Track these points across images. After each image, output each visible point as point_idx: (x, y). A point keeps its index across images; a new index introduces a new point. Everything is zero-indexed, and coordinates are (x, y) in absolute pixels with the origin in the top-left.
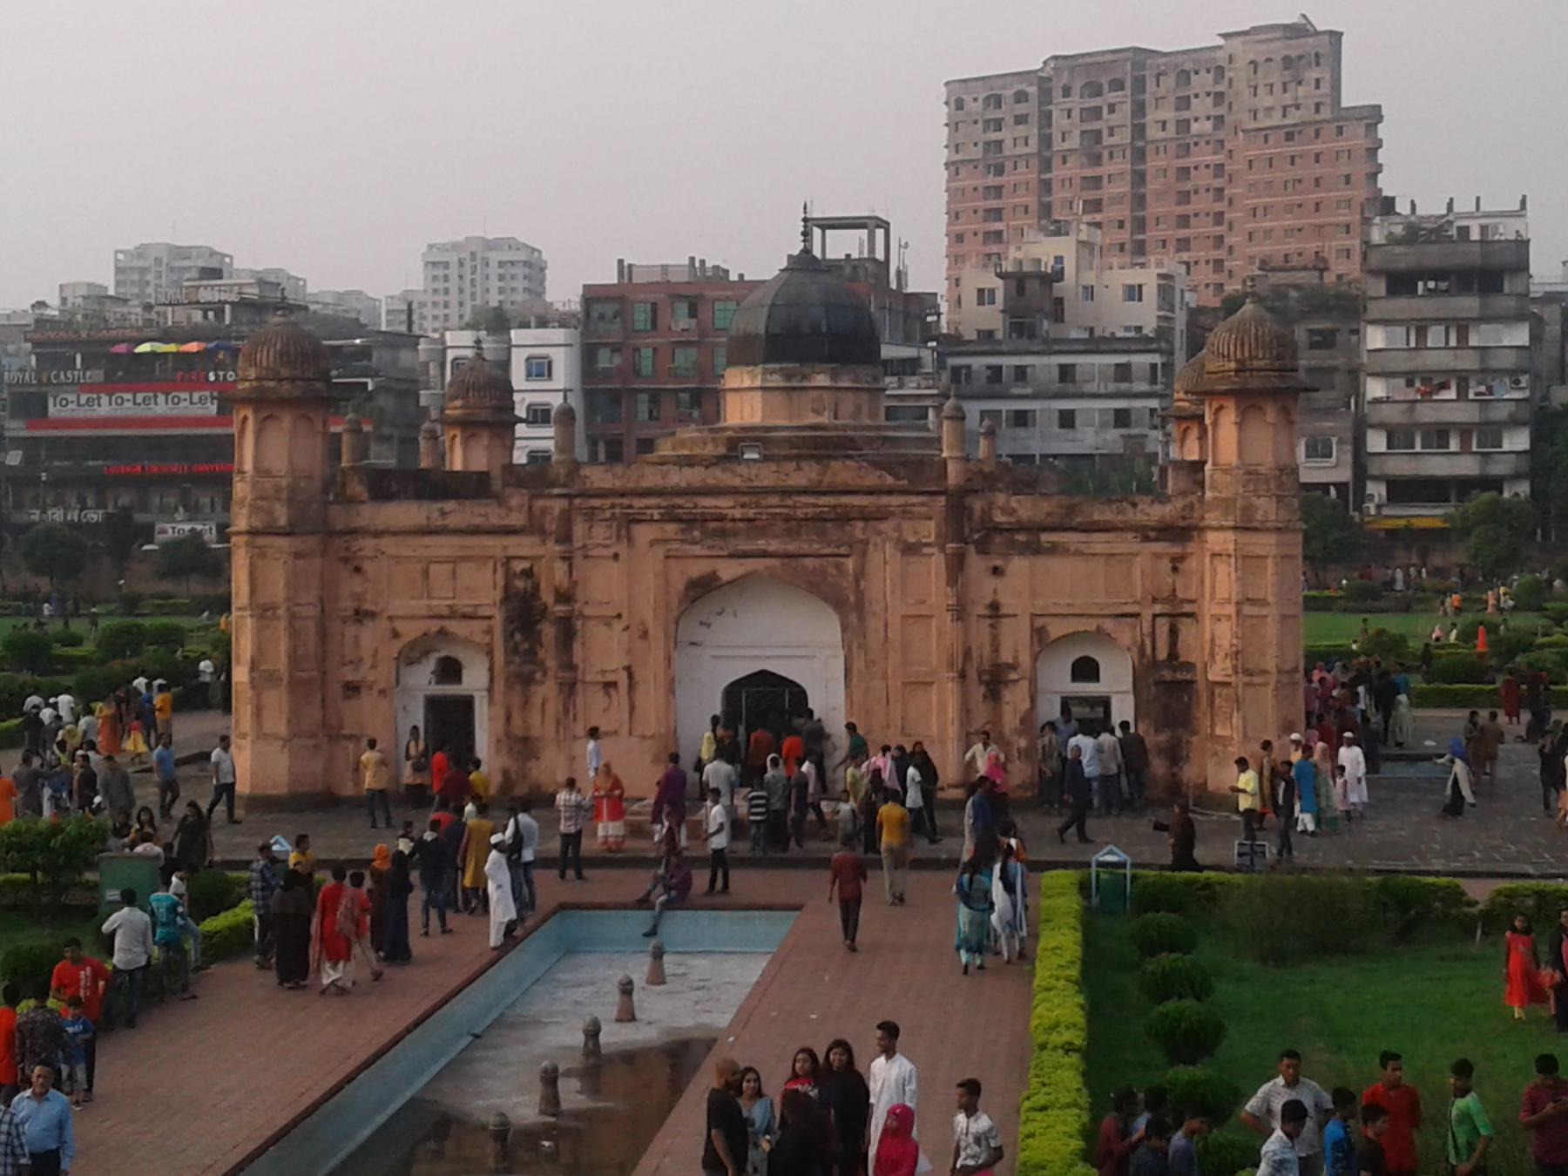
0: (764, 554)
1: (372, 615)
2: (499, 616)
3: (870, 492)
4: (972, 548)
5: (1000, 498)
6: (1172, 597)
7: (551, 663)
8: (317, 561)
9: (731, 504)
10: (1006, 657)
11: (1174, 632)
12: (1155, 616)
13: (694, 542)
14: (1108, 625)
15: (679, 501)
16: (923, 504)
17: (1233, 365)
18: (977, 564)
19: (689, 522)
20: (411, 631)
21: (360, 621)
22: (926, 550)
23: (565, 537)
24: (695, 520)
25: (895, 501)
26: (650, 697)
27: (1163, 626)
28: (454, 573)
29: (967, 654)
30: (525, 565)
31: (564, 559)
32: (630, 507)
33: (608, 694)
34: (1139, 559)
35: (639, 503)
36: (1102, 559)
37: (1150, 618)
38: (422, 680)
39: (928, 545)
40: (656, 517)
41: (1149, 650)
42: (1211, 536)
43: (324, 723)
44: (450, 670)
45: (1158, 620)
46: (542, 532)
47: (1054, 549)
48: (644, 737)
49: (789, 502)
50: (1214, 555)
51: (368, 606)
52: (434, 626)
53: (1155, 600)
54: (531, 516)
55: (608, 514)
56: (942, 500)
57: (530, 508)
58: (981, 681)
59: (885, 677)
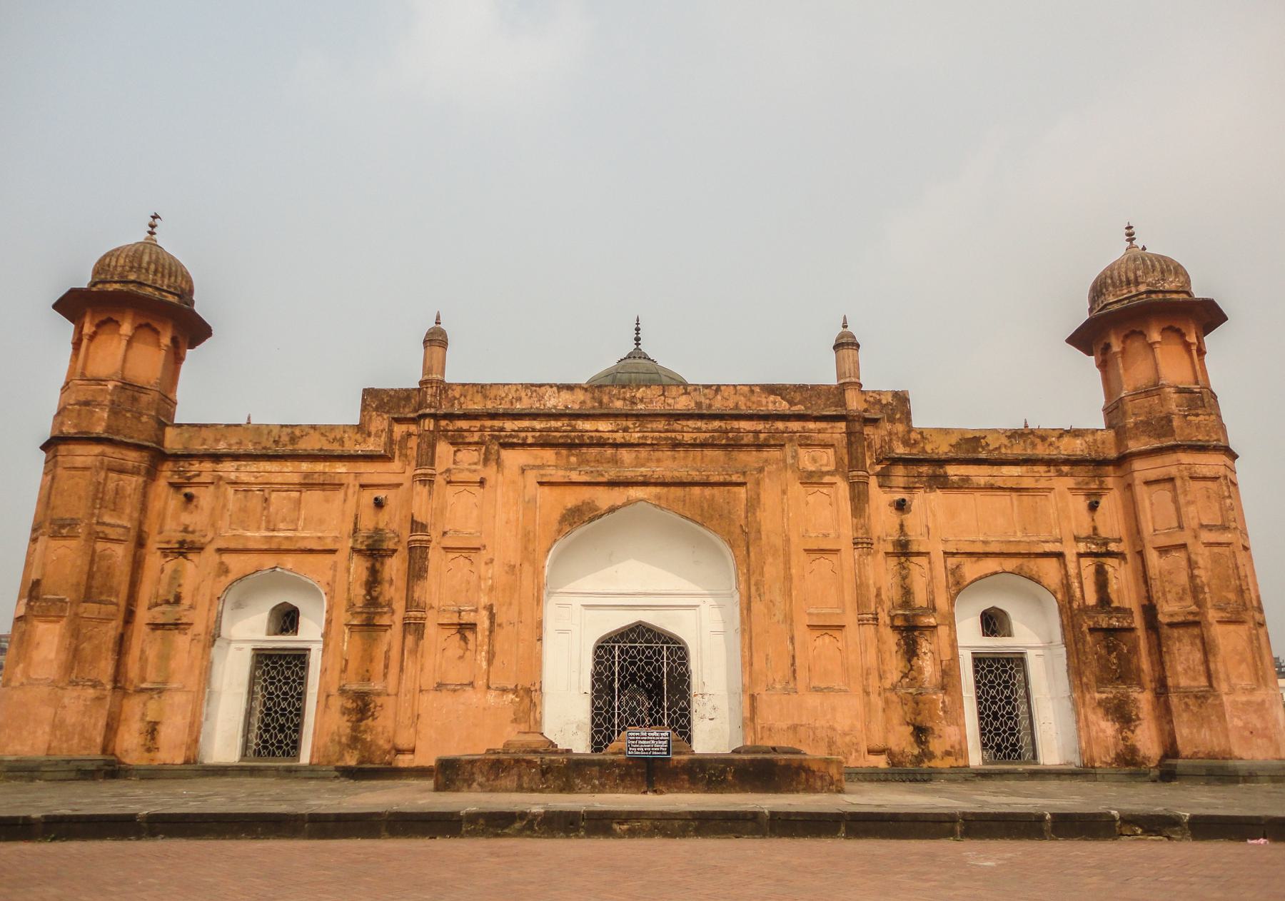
4: (873, 482)
5: (900, 428)
6: (1094, 536)
7: (399, 606)
11: (1101, 574)
12: (1080, 555)
15: (553, 424)
17: (1143, 288)
21: (181, 554)
22: (827, 479)
27: (1088, 566)
28: (299, 501)
29: (878, 595)
30: (381, 494)
31: (423, 482)
32: (502, 429)
33: (464, 639)
34: (1051, 495)
35: (509, 425)
36: (1014, 495)
37: (1074, 559)
38: (249, 629)
39: (828, 473)
40: (530, 441)
41: (1078, 594)
42: (1138, 465)
44: (287, 619)
45: (1082, 560)
47: (964, 485)
48: (504, 690)
50: (1147, 483)
53: (1077, 539)
54: (391, 441)
55: (476, 438)
57: (391, 431)
58: (894, 628)
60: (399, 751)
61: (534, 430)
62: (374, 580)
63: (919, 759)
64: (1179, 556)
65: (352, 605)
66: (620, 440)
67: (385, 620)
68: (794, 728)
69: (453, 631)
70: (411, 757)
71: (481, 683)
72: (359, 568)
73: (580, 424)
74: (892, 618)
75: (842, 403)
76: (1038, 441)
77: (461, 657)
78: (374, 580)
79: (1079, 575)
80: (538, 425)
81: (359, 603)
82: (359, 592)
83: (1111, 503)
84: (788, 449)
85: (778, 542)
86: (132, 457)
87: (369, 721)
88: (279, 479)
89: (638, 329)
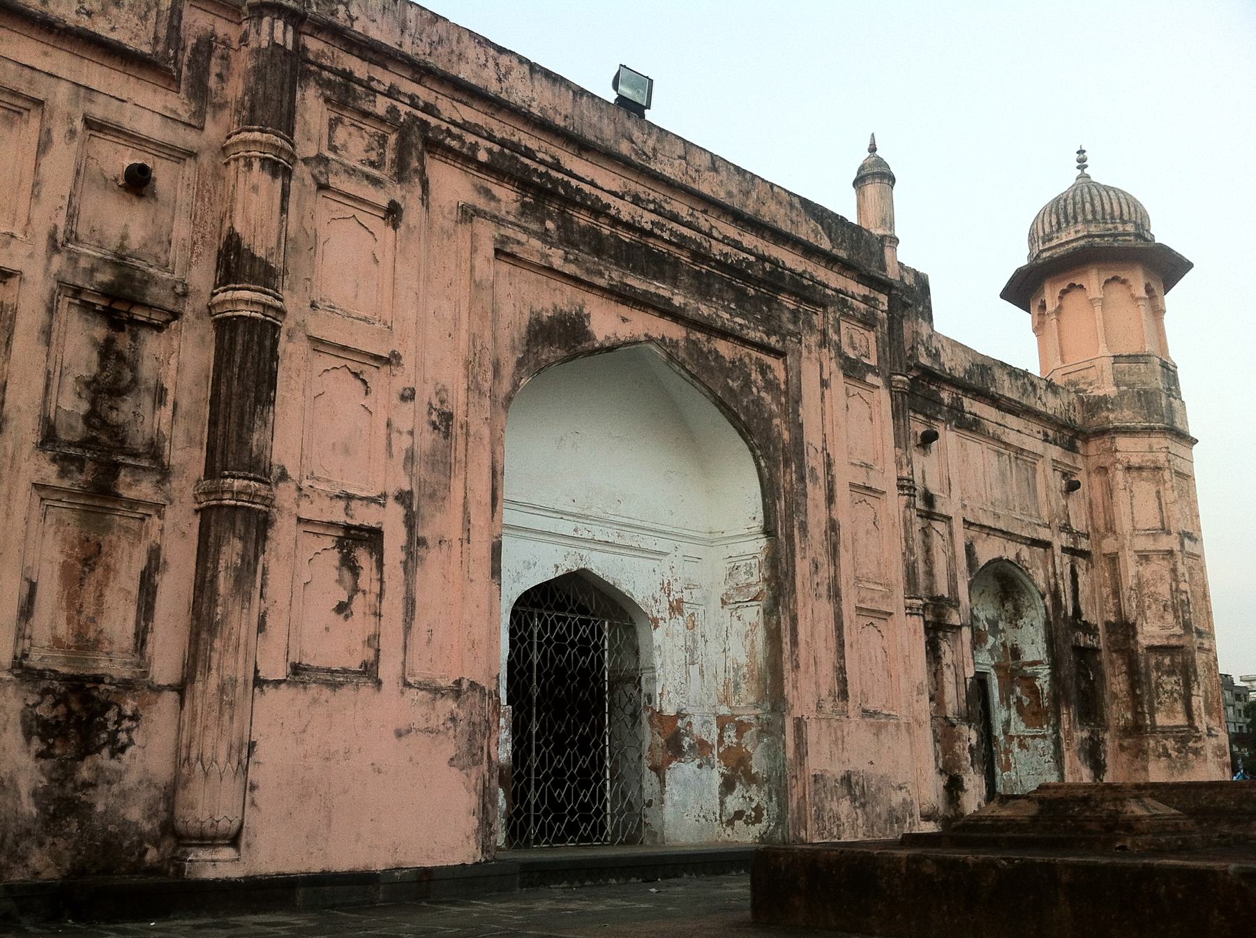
3: (810, 251)
7: (187, 457)
9: (614, 187)
10: (942, 589)
14: (1025, 553)
16: (865, 299)
22: (870, 378)
24: (552, 194)
32: (429, 109)
33: (349, 564)
39: (870, 369)
40: (483, 156)
42: (1122, 442)
46: (200, 92)
49: (705, 226)
50: (1129, 468)
55: (381, 106)
59: (835, 594)
60: (179, 837)
61: (490, 138)
62: (112, 382)
64: (1159, 567)
65: (49, 437)
66: (625, 217)
67: (145, 489)
68: (847, 780)
69: (329, 542)
70: (227, 853)
71: (388, 670)
77: (342, 608)
78: (112, 382)
83: (1091, 486)
87: (104, 759)
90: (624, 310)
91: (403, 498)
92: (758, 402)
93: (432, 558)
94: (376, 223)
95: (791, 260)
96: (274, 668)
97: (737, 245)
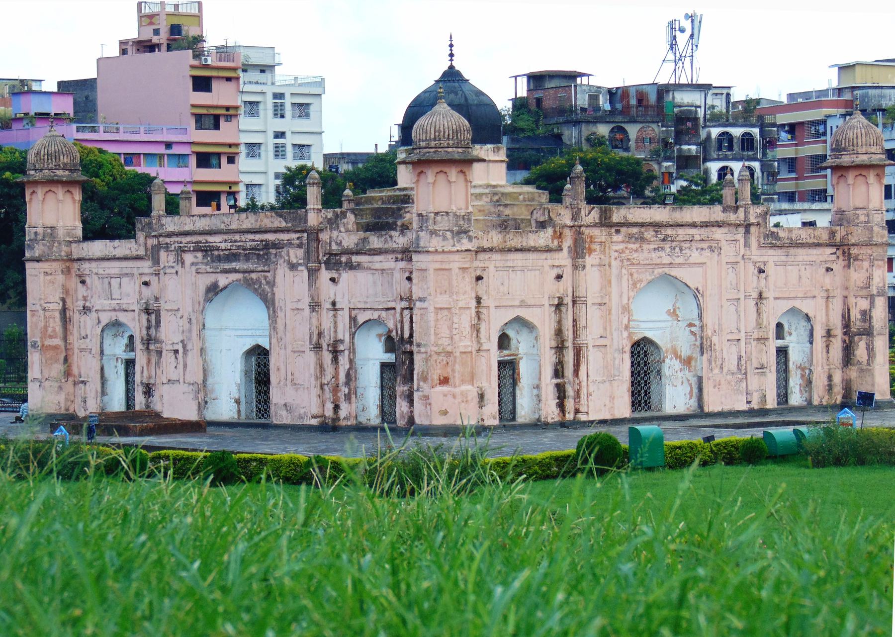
0: (235, 271)
1: (89, 310)
2: (136, 307)
3: (276, 231)
4: (323, 265)
5: (335, 234)
8: (61, 278)
10: (340, 337)
13: (207, 264)
14: (384, 314)
16: (298, 238)
18: (325, 275)
19: (206, 250)
20: (105, 318)
22: (300, 268)
23: (156, 261)
25: (284, 237)
26: (193, 360)
29: (320, 335)
35: (185, 240)
38: (117, 348)
39: (300, 264)
41: (399, 332)
43: (68, 374)
49: (244, 239)
51: (87, 304)
52: (113, 316)
53: (402, 299)
54: (146, 250)
56: (305, 235)
63: (334, 420)
65: (142, 339)
68: (285, 405)
71: (181, 380)
72: (144, 317)
73: (211, 239)
74: (328, 345)
75: (306, 222)
76: (389, 239)
79: (402, 322)
80: (194, 239)
81: (145, 337)
82: (145, 332)
84: (285, 250)
85: (282, 304)
86: (55, 265)
88: (113, 271)
89: (451, 46)
90: (227, 275)
91: (182, 341)
92: (263, 290)
93: (190, 354)
94: (175, 276)
95: (271, 237)
96: (165, 381)
97: (254, 240)
